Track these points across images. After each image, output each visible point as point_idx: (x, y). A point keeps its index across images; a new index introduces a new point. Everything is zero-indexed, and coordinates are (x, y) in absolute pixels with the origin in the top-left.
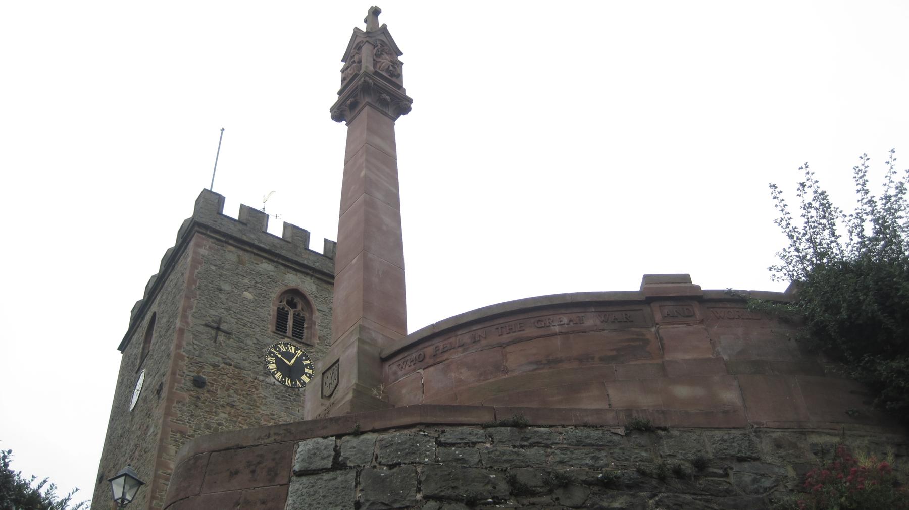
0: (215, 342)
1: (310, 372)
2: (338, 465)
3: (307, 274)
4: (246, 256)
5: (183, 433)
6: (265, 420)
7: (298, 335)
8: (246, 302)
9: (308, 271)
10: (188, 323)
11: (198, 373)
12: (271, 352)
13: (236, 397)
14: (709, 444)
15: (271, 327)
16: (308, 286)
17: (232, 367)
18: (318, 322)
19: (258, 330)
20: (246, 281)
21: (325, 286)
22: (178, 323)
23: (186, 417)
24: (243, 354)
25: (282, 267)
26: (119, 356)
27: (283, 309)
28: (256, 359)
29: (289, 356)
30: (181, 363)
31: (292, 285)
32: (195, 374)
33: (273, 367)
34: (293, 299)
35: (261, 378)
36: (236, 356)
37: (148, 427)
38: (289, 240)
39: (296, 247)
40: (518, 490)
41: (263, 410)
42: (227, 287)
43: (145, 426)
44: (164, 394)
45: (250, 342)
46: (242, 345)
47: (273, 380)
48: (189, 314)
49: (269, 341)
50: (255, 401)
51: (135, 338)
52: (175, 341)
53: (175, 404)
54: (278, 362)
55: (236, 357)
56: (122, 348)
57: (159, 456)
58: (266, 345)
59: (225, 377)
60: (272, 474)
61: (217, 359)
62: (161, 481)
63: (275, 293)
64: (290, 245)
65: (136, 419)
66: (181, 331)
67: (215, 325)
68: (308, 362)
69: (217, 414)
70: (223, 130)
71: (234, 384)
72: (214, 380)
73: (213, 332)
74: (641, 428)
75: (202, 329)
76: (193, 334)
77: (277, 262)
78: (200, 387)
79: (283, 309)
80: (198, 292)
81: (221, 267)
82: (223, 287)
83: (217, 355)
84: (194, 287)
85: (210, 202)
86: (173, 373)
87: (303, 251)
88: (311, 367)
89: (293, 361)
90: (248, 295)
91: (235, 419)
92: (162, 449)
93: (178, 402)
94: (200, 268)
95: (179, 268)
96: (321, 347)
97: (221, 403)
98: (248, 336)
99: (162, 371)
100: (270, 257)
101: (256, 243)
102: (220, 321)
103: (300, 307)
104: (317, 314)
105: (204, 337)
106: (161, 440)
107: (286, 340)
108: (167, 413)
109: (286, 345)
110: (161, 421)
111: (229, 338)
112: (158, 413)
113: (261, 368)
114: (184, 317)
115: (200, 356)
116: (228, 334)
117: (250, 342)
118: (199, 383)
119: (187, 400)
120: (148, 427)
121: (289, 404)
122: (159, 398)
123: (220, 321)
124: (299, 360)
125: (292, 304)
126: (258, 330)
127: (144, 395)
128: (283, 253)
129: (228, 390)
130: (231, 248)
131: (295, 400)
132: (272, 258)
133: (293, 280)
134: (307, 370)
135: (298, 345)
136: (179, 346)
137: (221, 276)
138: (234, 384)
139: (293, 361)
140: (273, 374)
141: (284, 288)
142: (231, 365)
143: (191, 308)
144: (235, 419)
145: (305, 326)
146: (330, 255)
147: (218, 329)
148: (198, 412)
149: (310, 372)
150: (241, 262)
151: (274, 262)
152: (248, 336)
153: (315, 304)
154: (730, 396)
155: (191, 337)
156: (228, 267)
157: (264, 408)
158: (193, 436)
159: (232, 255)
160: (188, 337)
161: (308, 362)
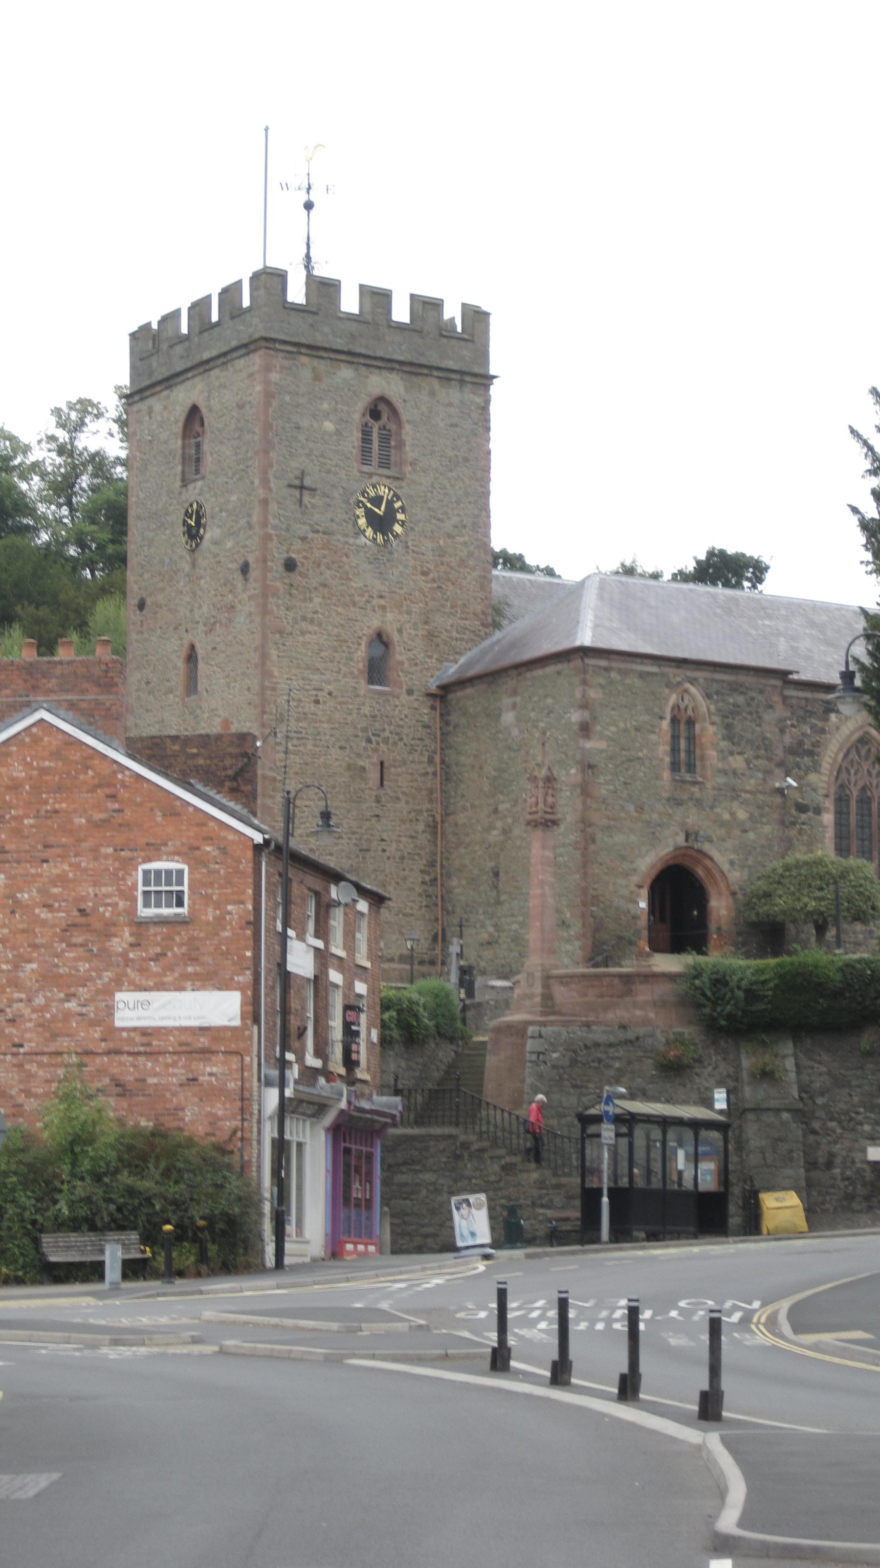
0: (301, 505)
2: (540, 1036)
3: (392, 369)
4: (321, 366)
5: (281, 632)
7: (385, 463)
10: (270, 490)
11: (288, 552)
14: (642, 1031)
20: (325, 406)
21: (415, 379)
22: (261, 492)
31: (376, 392)
32: (285, 555)
33: (362, 522)
35: (351, 541)
38: (369, 318)
40: (586, 1047)
41: (357, 584)
42: (305, 423)
46: (328, 500)
47: (363, 539)
51: (156, 404)
54: (369, 514)
60: (523, 1036)
62: (268, 692)
67: (297, 482)
69: (311, 599)
70: (267, 129)
71: (325, 557)
73: (297, 493)
74: (623, 1027)
76: (279, 503)
79: (366, 425)
83: (304, 523)
88: (403, 509)
89: (383, 507)
90: (329, 426)
93: (273, 595)
94: (275, 403)
97: (315, 584)
102: (302, 475)
104: (407, 428)
113: (350, 527)
114: (265, 481)
116: (313, 490)
118: (290, 566)
122: (246, 580)
123: (302, 475)
124: (390, 503)
131: (388, 560)
136: (265, 524)
138: (325, 557)
139: (383, 507)
143: (271, 466)
145: (393, 443)
147: (302, 488)
150: (317, 378)
152: (333, 486)
153: (405, 415)
154: (652, 1015)
160: (273, 507)
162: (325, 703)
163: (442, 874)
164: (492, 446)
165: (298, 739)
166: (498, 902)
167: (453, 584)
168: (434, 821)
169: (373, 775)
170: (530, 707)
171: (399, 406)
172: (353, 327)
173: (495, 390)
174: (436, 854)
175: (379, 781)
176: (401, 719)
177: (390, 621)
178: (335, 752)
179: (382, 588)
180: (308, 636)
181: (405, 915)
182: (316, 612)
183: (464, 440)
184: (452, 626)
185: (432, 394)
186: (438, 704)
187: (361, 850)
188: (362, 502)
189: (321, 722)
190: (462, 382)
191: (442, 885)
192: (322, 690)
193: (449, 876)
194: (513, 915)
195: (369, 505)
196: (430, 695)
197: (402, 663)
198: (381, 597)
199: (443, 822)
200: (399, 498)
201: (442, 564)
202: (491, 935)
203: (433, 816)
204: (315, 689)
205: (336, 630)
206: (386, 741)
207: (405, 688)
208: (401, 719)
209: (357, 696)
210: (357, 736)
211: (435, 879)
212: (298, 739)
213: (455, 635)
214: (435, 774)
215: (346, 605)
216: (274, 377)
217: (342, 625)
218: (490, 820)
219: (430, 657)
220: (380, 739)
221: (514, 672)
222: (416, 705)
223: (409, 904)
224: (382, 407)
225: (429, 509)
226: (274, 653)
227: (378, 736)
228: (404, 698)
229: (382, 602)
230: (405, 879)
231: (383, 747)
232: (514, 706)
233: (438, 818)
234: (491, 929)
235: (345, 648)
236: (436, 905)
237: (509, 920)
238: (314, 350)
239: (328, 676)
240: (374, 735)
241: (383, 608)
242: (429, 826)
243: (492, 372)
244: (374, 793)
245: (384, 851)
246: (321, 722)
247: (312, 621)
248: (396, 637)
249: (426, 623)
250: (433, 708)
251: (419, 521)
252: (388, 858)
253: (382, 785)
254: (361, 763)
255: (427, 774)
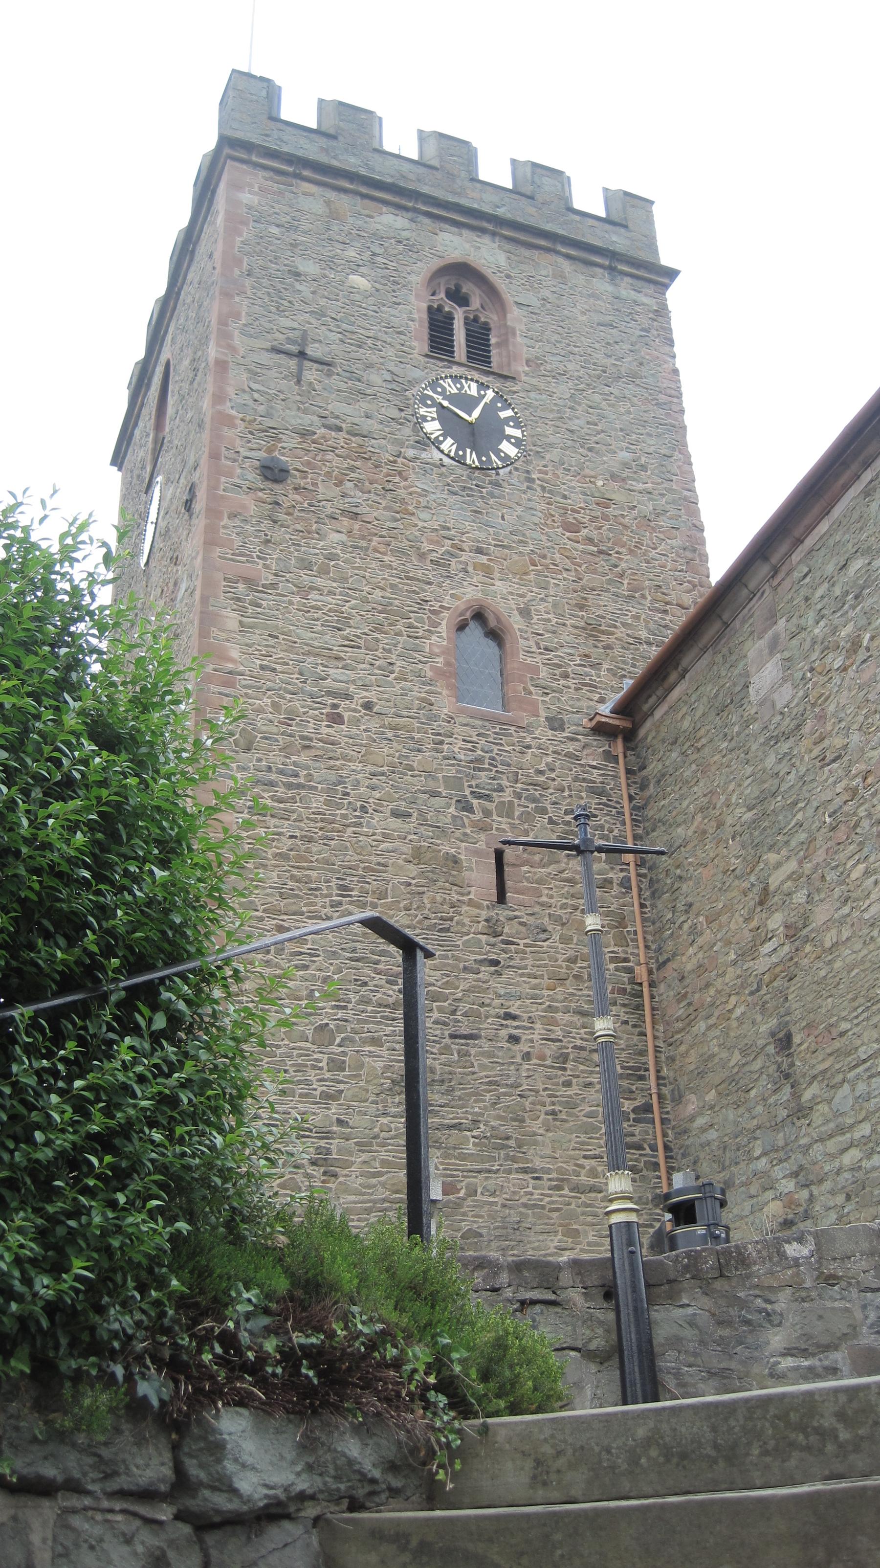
0: (299, 382)
1: (517, 433)
3: (483, 231)
4: (344, 202)
6: (431, 542)
8: (358, 297)
9: (485, 225)
10: (233, 349)
11: (269, 451)
12: (424, 399)
13: (359, 497)
15: (420, 345)
16: (488, 255)
17: (343, 434)
18: (520, 328)
19: (390, 352)
20: (351, 253)
21: (527, 253)
23: (255, 548)
24: (364, 405)
25: (427, 221)
26: (115, 477)
27: (440, 309)
28: (395, 413)
29: (469, 403)
30: (228, 433)
32: (262, 454)
33: (433, 427)
34: (458, 288)
35: (411, 453)
36: (349, 410)
37: (175, 584)
38: (435, 163)
39: (451, 176)
43: (172, 581)
44: (199, 505)
45: (376, 378)
47: (437, 455)
48: (234, 328)
49: (418, 373)
50: (403, 501)
52: (210, 388)
53: (225, 521)
54: (444, 415)
55: (352, 412)
56: (118, 460)
57: (204, 633)
58: (413, 383)
59: (330, 456)
61: (308, 420)
63: (417, 274)
64: (438, 175)
65: (154, 579)
66: (222, 366)
67: (294, 349)
68: (509, 413)
69: (321, 536)
72: (308, 464)
73: (293, 363)
75: (265, 358)
76: (250, 371)
77: (415, 210)
78: (276, 481)
79: (440, 309)
80: (248, 282)
81: (291, 228)
82: (301, 269)
83: (305, 411)
84: (237, 272)
85: (249, 96)
86: (215, 456)
87: (469, 184)
89: (476, 413)
91: (363, 543)
92: (208, 620)
93: (232, 516)
95: (202, 249)
96: (534, 381)
97: (329, 511)
98: (370, 366)
99: (191, 462)
100: (397, 200)
101: (363, 172)
103: (475, 303)
104: (516, 317)
105: (273, 373)
106: (204, 600)
107: (455, 370)
108: (210, 542)
109: (456, 379)
110: (199, 561)
111: (329, 374)
112: (192, 547)
113: (407, 431)
114: (224, 335)
115: (268, 415)
117: (376, 378)
118: (273, 473)
119: (252, 509)
120: (175, 584)
121: (480, 503)
125: (462, 300)
126: (390, 352)
127: (162, 524)
128: (425, 189)
129: (339, 483)
130: (306, 186)
131: (492, 496)
132: (403, 202)
133: (455, 245)
134: (509, 431)
135: (484, 379)
136: (219, 398)
137: (294, 245)
138: (353, 469)
139: (476, 413)
140: (437, 444)
141: (436, 264)
142: (340, 429)
143: (237, 316)
144: (363, 543)
145: (493, 340)
146: (528, 189)
147: (302, 355)
148: (278, 534)
149: (517, 433)
150: (334, 215)
151: (406, 209)
152: (370, 366)
155: (245, 376)
156: (306, 226)
157: (424, 515)
158: (274, 586)
159: (312, 200)
160: (237, 377)
161: (509, 413)
162: (357, 722)
163: (660, 1096)
164: (680, 363)
165: (289, 786)
166: (800, 1112)
167: (631, 552)
168: (632, 981)
169: (481, 878)
170: (811, 615)
171: (498, 281)
172: (406, 167)
173: (674, 295)
174: (643, 1053)
175: (494, 891)
176: (541, 773)
177: (503, 596)
178: (380, 822)
179: (482, 536)
180: (314, 595)
181: (576, 1189)
182: (331, 557)
183: (626, 346)
184: (637, 618)
185: (561, 277)
186: (619, 747)
187: (453, 1036)
188: (431, 398)
189: (345, 757)
190: (611, 269)
191: (663, 1121)
192: (348, 697)
193: (678, 1099)
194: (841, 1130)
195: (446, 403)
196: (601, 730)
197: (535, 670)
198: (480, 551)
199: (652, 985)
200: (508, 405)
201: (605, 518)
202: (790, 1202)
203: (630, 970)
204: (329, 693)
205: (378, 593)
206: (506, 810)
207: (543, 714)
208: (541, 773)
209: (435, 718)
210: (435, 794)
211: (647, 1108)
212: (289, 786)
213: (644, 634)
214: (625, 884)
215: (400, 553)
216: (247, 197)
217: (392, 586)
218: (754, 923)
219: (596, 666)
220: (491, 806)
221: (763, 570)
222: (571, 747)
223: (587, 1163)
224: (468, 287)
225: (571, 431)
226: (231, 619)
227: (488, 798)
228: (543, 733)
229: (484, 559)
230: (571, 1105)
231: (500, 822)
232: (774, 646)
233: (641, 973)
234: (788, 1186)
235: (399, 627)
236: (656, 1166)
237: (832, 1146)
238: (327, 174)
239: (362, 672)
240: (479, 796)
241: (487, 571)
242: (623, 991)
243: (666, 259)
244: (484, 914)
245: (514, 1039)
246: (345, 757)
247: (324, 571)
248: (516, 622)
249: (581, 607)
250: (610, 757)
251: (551, 445)
252: (527, 1056)
253: (501, 898)
254: (447, 848)
255: (610, 882)
